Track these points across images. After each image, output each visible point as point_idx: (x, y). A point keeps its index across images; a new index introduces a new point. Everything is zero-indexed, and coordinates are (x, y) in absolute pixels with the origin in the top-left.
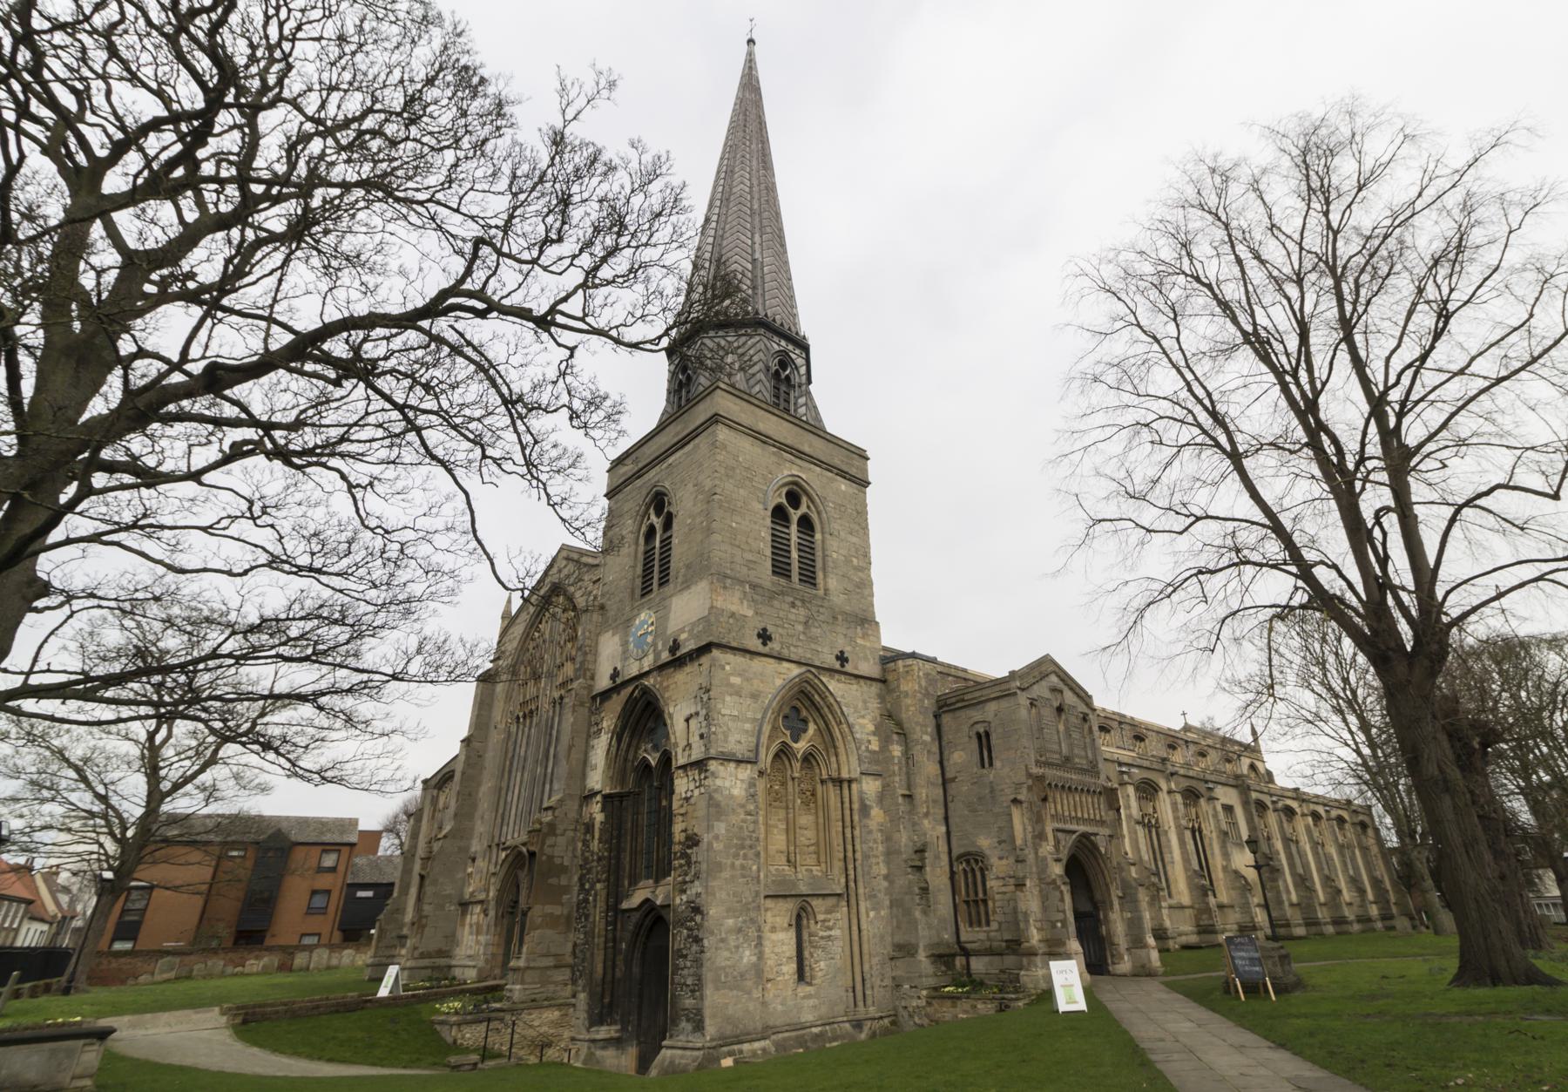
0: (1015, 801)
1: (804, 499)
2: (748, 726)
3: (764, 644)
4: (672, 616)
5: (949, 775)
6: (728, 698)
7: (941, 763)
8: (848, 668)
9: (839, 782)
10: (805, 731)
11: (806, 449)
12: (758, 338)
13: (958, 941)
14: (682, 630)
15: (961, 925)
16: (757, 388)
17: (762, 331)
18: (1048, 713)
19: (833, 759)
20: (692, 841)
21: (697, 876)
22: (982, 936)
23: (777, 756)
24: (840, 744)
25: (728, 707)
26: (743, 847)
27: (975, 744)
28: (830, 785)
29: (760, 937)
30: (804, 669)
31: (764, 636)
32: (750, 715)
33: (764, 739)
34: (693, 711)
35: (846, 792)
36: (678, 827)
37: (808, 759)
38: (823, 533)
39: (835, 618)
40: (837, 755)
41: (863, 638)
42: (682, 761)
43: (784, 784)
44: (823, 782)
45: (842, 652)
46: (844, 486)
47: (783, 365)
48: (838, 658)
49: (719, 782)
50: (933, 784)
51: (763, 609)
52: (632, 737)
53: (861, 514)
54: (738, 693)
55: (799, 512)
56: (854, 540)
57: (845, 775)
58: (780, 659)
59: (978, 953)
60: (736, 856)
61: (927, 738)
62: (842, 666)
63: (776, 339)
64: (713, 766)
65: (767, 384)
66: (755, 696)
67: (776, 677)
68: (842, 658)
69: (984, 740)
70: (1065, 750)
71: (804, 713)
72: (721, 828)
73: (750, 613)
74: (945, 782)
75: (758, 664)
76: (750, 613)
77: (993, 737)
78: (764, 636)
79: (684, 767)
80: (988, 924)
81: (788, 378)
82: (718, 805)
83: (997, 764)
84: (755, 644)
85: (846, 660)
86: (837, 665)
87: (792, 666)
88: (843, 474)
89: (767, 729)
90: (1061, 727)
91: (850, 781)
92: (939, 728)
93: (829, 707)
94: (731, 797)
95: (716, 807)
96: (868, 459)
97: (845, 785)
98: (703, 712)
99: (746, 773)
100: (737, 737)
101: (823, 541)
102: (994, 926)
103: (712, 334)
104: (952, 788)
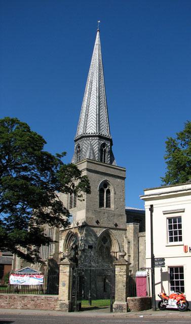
4: (77, 216)
8: (118, 227)
10: (107, 241)
11: (109, 172)
14: (79, 220)
29: (96, 283)
31: (98, 222)
51: (97, 215)
58: (101, 227)
68: (116, 225)
73: (94, 217)
76: (94, 217)
78: (98, 222)
84: (95, 224)
103: (86, 139)
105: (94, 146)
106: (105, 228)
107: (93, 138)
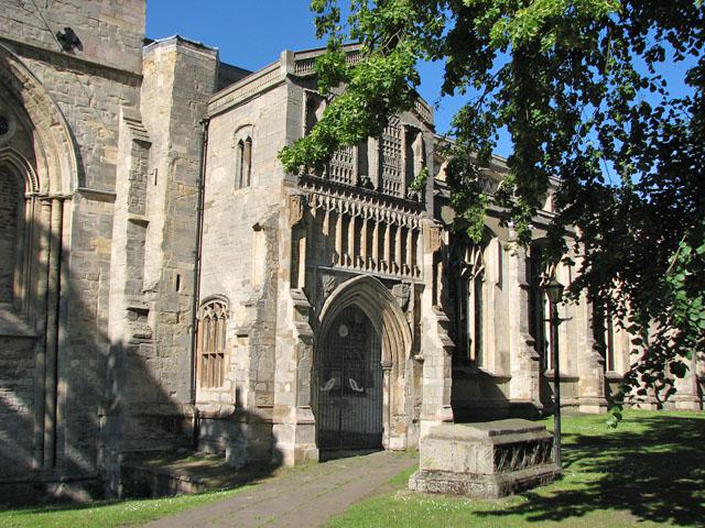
8: (78, 54)
22: (215, 397)
40: (46, 165)
41: (113, 15)
48: (61, 38)
50: (180, 209)
57: (53, 192)
68: (69, 39)
69: (245, 146)
77: (255, 143)
83: (255, 180)
85: (78, 43)
86: (57, 47)
91: (62, 200)
97: (56, 204)
104: (207, 213)
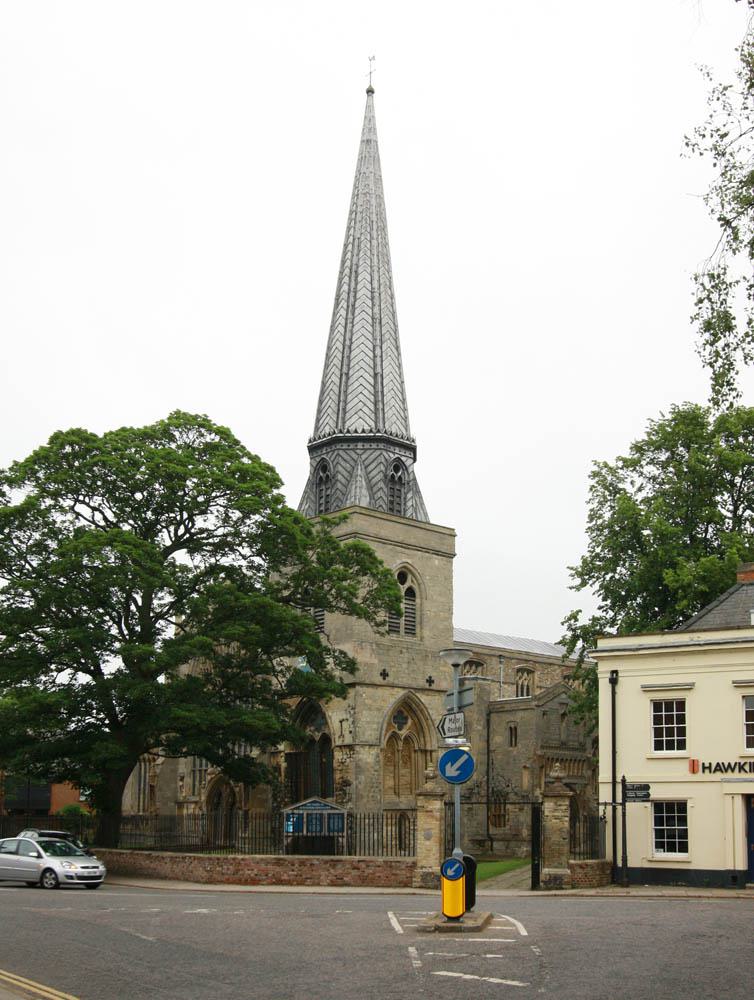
0: (525, 767)
1: (410, 577)
2: (375, 726)
3: (384, 679)
5: (492, 748)
6: (364, 712)
7: (488, 741)
8: (434, 687)
9: (425, 752)
10: (406, 723)
11: (412, 541)
12: (378, 452)
13: (488, 834)
15: (490, 827)
16: (379, 494)
17: (381, 446)
18: (554, 717)
19: (422, 739)
20: (347, 783)
21: (350, 800)
22: (501, 832)
23: (390, 738)
24: (426, 731)
25: (365, 717)
26: (372, 787)
27: (508, 733)
28: (419, 754)
30: (406, 691)
31: (384, 674)
32: (376, 720)
33: (384, 732)
34: (344, 717)
35: (429, 758)
36: (337, 776)
37: (407, 739)
38: (421, 598)
39: (427, 656)
40: (424, 737)
42: (339, 742)
43: (393, 753)
44: (415, 751)
45: (430, 677)
46: (437, 561)
47: (396, 469)
49: (361, 756)
52: (301, 723)
53: (449, 578)
54: (370, 709)
55: (406, 586)
56: (442, 599)
57: (429, 748)
58: (393, 686)
59: (498, 840)
60: (370, 791)
61: (480, 728)
62: (430, 685)
63: (392, 449)
64: (357, 748)
65: (385, 490)
66: (379, 710)
67: (390, 698)
68: (430, 681)
70: (563, 737)
71: (406, 714)
72: (362, 778)
73: (376, 661)
74: (488, 753)
75: (380, 692)
77: (519, 731)
79: (340, 747)
80: (505, 826)
81: (400, 478)
82: (359, 767)
83: (519, 746)
84: (379, 680)
87: (399, 690)
88: (437, 553)
89: (385, 725)
90: (564, 724)
91: (431, 752)
92: (488, 721)
93: (422, 711)
94: (367, 763)
95: (359, 769)
96: (455, 536)
97: (429, 754)
98: (351, 720)
99: (374, 751)
100: (369, 732)
101: (421, 605)
102: (508, 827)
103: (345, 446)
105: (370, 469)
106: (404, 688)
107: (367, 446)
